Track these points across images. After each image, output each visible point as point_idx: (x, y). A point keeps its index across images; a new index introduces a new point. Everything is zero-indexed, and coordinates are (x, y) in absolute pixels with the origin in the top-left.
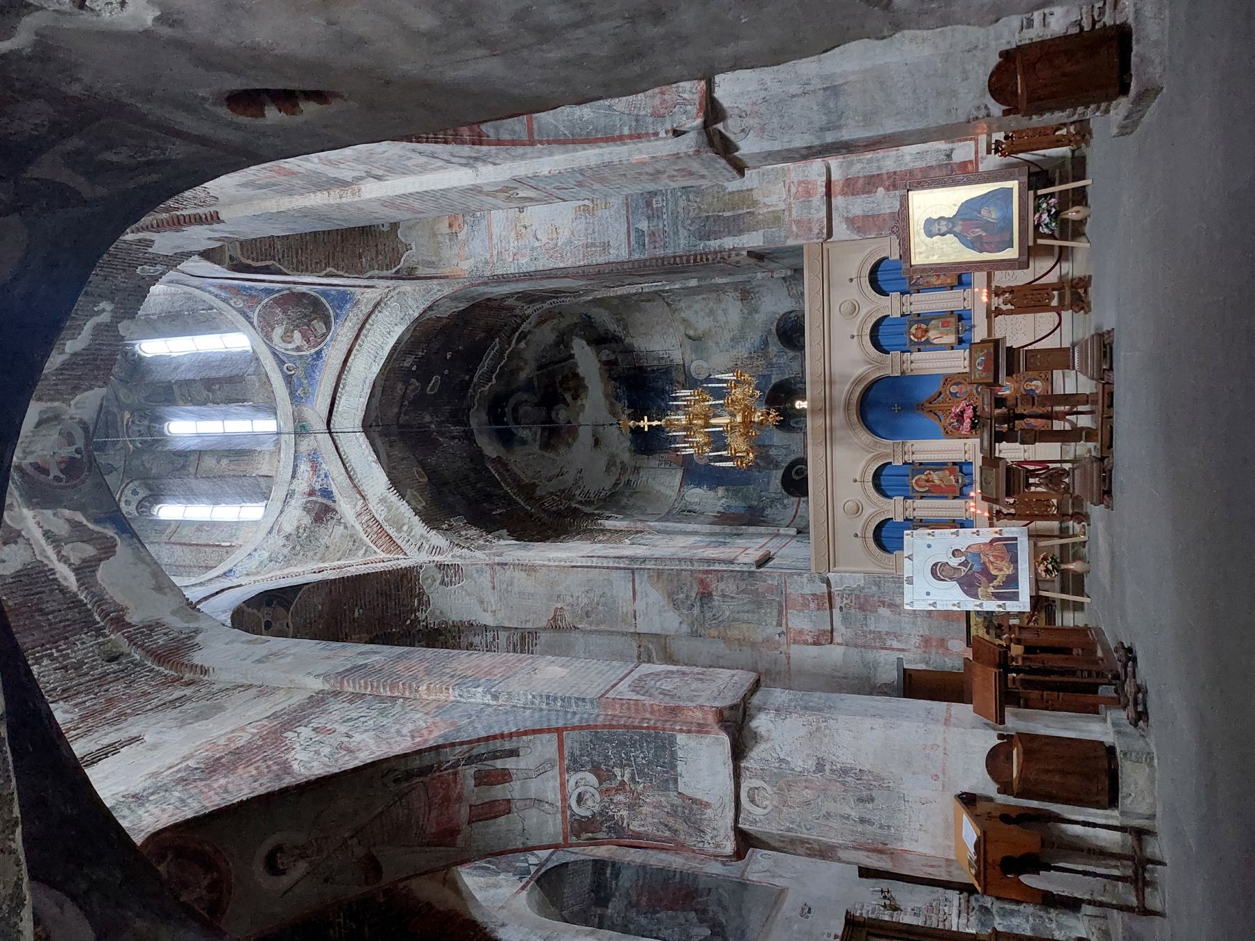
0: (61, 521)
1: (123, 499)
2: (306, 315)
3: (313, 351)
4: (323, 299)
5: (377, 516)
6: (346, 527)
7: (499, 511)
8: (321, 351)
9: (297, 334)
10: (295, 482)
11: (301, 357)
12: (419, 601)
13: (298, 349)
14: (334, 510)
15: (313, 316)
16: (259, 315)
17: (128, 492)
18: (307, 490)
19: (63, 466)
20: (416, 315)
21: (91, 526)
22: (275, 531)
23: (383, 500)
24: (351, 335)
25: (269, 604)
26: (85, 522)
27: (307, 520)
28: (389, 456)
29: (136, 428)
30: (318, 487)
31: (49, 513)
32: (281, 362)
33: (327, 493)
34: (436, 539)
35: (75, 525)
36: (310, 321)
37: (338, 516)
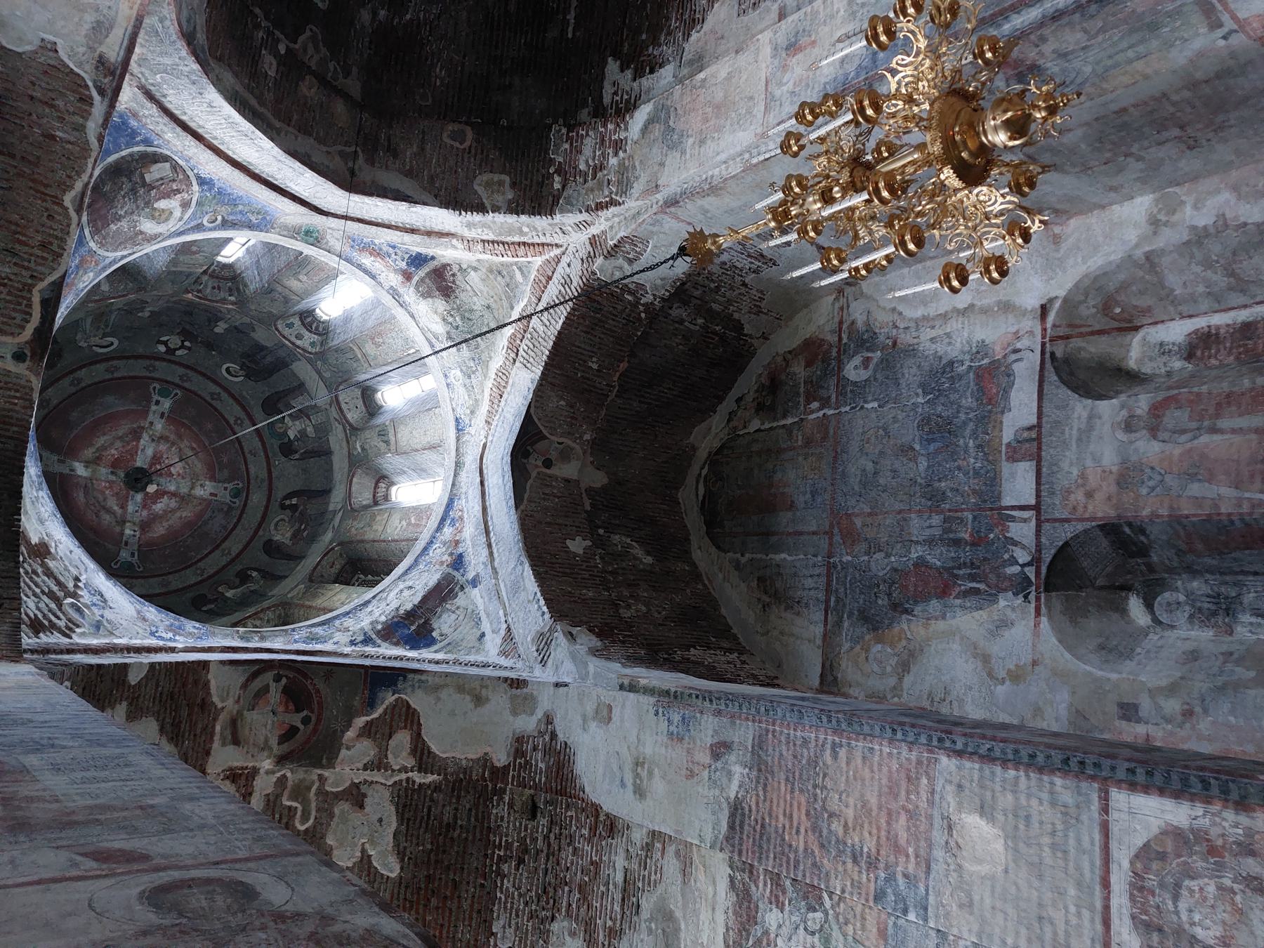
0: (358, 745)
1: (293, 339)
2: (134, 191)
3: (196, 187)
4: (111, 159)
5: (485, 238)
6: (475, 269)
7: (571, 17)
8: (198, 177)
9: (162, 204)
10: (382, 278)
11: (199, 204)
12: (630, 293)
13: (185, 205)
14: (445, 266)
15: (136, 178)
16: (115, 251)
17: (286, 332)
18: (400, 278)
19: (291, 707)
20: (196, 67)
21: (375, 715)
22: (434, 341)
23: (470, 226)
24: (189, 141)
25: (527, 455)
26: (368, 718)
27: (441, 304)
28: (409, 174)
29: (208, 290)
30: (403, 265)
31: (344, 752)
32: (199, 228)
33: (418, 260)
34: (568, 219)
35: (368, 731)
36: (144, 184)
37: (455, 269)
